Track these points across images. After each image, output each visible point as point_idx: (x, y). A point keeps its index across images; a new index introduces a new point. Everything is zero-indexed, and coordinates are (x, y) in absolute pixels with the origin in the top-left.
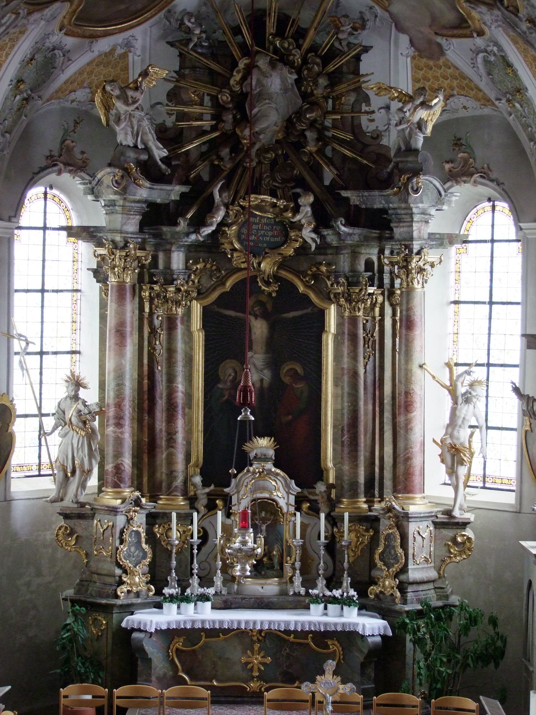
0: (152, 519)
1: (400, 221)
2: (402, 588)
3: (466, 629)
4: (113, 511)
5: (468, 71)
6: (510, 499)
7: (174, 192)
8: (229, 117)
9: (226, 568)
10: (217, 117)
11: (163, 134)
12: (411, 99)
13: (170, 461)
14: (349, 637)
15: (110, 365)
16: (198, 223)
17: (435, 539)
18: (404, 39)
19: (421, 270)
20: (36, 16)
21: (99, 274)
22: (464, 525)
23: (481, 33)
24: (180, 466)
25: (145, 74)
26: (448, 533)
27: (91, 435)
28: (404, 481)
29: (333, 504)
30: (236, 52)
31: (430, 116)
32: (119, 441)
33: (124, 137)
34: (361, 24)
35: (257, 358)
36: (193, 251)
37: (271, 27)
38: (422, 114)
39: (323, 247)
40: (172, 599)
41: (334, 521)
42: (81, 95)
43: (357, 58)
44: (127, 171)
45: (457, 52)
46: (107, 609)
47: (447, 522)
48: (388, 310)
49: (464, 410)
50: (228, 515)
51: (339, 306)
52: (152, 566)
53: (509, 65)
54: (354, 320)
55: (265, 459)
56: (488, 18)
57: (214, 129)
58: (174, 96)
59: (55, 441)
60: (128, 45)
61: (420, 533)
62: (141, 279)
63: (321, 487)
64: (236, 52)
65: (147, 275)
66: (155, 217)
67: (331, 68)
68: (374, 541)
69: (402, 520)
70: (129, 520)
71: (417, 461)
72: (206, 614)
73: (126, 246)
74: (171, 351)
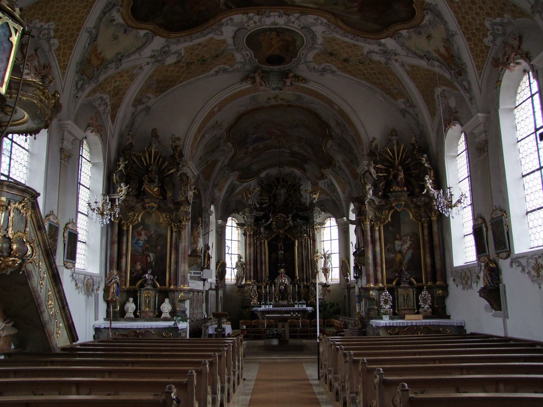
0: (259, 288)
1: (311, 218)
3: (331, 307)
4: (249, 285)
5: (323, 188)
10: (270, 200)
12: (312, 193)
13: (262, 275)
15: (248, 252)
16: (266, 221)
18: (309, 182)
19: (316, 229)
20: (232, 174)
21: (245, 234)
23: (326, 178)
24: (264, 276)
25: (254, 189)
27: (244, 269)
30: (273, 186)
32: (250, 269)
36: (266, 228)
37: (281, 180)
38: (315, 196)
39: (295, 226)
40: (263, 304)
41: (299, 287)
44: (251, 208)
45: (321, 184)
47: (325, 286)
49: (327, 260)
50: (275, 287)
51: (298, 239)
52: (258, 298)
54: (302, 242)
57: (269, 202)
60: (250, 185)
64: (273, 186)
65: (255, 234)
66: (257, 220)
68: (309, 291)
70: (253, 287)
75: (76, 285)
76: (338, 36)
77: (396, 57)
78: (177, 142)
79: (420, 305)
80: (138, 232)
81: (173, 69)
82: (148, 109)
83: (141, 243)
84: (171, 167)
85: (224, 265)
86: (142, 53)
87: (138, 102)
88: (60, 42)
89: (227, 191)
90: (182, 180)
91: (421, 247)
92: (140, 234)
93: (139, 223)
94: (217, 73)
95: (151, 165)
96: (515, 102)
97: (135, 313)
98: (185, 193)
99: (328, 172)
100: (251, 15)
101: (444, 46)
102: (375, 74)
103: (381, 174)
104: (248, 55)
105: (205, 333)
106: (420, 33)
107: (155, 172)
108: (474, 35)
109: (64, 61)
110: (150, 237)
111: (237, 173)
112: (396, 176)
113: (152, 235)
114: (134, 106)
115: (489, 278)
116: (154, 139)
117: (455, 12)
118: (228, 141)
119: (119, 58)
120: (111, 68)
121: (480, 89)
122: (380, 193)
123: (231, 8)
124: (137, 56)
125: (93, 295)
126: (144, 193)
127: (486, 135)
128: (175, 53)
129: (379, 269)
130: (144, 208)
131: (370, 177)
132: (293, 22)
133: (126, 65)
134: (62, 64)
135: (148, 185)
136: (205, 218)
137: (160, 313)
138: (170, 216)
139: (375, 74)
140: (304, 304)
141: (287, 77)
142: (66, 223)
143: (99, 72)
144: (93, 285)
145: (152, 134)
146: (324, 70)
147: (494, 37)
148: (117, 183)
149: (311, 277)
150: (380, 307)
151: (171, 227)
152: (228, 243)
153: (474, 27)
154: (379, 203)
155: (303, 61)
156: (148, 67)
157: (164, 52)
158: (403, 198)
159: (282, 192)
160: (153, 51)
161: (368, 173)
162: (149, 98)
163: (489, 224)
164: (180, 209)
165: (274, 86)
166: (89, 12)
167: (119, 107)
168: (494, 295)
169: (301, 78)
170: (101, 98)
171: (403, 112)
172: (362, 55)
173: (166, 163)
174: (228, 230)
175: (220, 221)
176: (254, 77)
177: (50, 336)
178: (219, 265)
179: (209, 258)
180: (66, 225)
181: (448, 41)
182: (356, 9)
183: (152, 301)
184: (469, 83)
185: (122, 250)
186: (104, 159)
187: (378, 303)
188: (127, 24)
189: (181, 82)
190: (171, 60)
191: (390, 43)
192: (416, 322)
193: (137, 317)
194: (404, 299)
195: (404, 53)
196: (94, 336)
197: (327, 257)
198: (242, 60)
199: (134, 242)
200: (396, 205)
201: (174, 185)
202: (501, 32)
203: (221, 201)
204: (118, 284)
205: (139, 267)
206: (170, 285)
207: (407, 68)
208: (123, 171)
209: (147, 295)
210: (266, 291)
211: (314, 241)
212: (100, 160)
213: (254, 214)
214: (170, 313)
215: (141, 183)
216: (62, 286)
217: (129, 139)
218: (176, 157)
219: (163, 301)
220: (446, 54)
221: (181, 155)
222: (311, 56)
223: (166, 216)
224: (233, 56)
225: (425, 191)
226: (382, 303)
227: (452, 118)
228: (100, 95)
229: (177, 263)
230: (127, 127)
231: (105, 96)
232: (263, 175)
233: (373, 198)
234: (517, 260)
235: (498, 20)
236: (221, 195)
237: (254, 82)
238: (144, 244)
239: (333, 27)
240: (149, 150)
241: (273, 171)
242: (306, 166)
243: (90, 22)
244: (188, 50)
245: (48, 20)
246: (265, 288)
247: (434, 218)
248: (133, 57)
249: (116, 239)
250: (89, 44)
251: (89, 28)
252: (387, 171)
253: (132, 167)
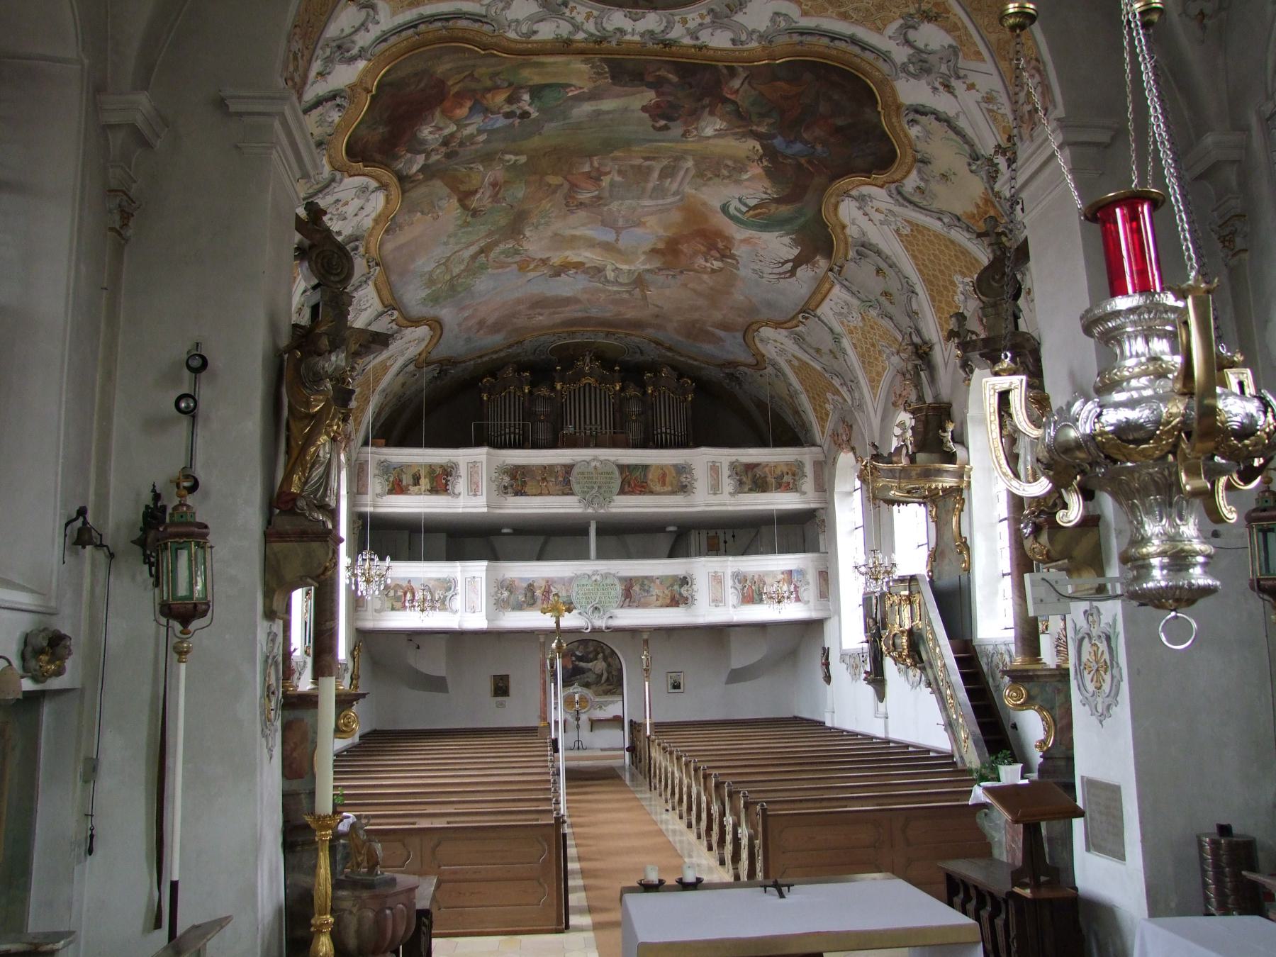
86: (951, 113)
100: (687, 41)
124: (962, 123)
128: (908, 42)
132: (587, 18)
160: (935, 89)
166: (925, 228)
182: (450, 83)
190: (932, 37)
244: (879, 23)
245: (953, 283)
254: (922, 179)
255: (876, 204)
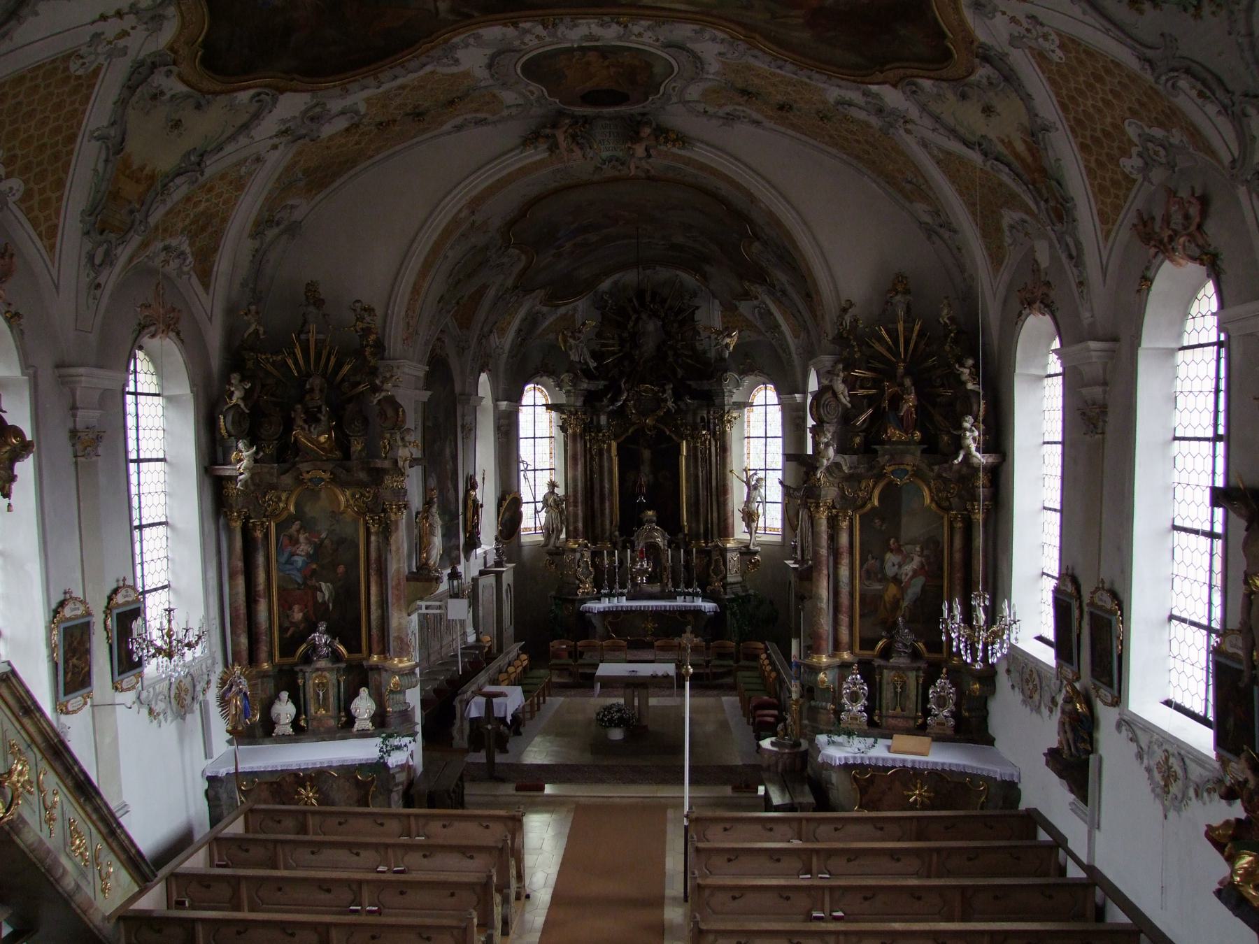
2: (724, 586)
4: (574, 550)
5: (750, 317)
6: (779, 539)
7: (601, 384)
8: (628, 345)
9: (633, 580)
11: (594, 355)
12: (722, 333)
14: (698, 612)
16: (613, 400)
17: (741, 561)
18: (717, 302)
21: (563, 428)
22: (755, 553)
23: (756, 298)
25: (584, 324)
26: (748, 557)
27: (561, 512)
28: (725, 530)
29: (687, 545)
31: (732, 341)
32: (576, 515)
33: (574, 357)
34: (694, 295)
35: (646, 469)
36: (611, 415)
37: (648, 299)
38: (728, 340)
39: (679, 411)
40: (605, 595)
42: (551, 336)
43: (693, 312)
44: (576, 374)
45: (744, 308)
46: (573, 601)
47: (746, 552)
48: (713, 443)
49: (754, 493)
50: (633, 551)
53: (772, 314)
54: (695, 448)
55: (651, 521)
56: (760, 290)
57: (620, 351)
58: (599, 335)
59: (543, 515)
60: (575, 309)
61: (733, 558)
62: (584, 431)
63: (681, 536)
66: (591, 399)
67: (680, 318)
69: (724, 551)
70: (582, 556)
71: (730, 521)
72: (624, 602)
73: (576, 413)
74: (601, 467)
75: (151, 711)
76: (757, 63)
77: (909, 126)
78: (368, 319)
79: (930, 710)
80: (290, 537)
81: (343, 141)
82: (293, 229)
83: (299, 560)
84: (358, 378)
85: (517, 502)
86: (253, 133)
87: (261, 226)
88: (26, 182)
89: (519, 331)
90: (383, 414)
91: (946, 574)
92: (294, 541)
93: (290, 515)
94: (458, 128)
95: (309, 375)
96: (1180, 335)
97: (295, 723)
98: (391, 448)
99: (757, 289)
101: (1025, 141)
102: (858, 142)
103: (861, 392)
104: (532, 93)
105: (462, 715)
106: (964, 97)
107: (321, 391)
108: (1096, 140)
109: (47, 219)
110: (318, 547)
111: (540, 293)
112: (896, 401)
113: (322, 541)
114: (257, 233)
115: (1070, 735)
116: (312, 309)
117: (1052, 82)
118: (507, 247)
119: (195, 162)
120: (178, 187)
121: (1104, 272)
122: (858, 440)
123: (469, 16)
124: (243, 140)
125: (197, 707)
126: (297, 448)
127: (1105, 392)
128: (343, 113)
129: (844, 619)
130: (299, 481)
131: (833, 404)
133: (213, 167)
134: (42, 228)
135: (303, 429)
136: (463, 416)
137: (351, 720)
138: (362, 495)
139: (858, 142)
140: (697, 595)
141: (635, 137)
142: (108, 592)
143: (144, 208)
144: (194, 686)
145: (307, 297)
146: (730, 118)
147: (1146, 164)
148: (230, 435)
149: (715, 532)
150: (839, 709)
151: (366, 523)
152: (525, 450)
153: (1099, 127)
154: (850, 468)
155: (674, 99)
156: (277, 153)
157: (312, 119)
158: (909, 459)
159: (651, 327)
160: (283, 121)
161: (828, 395)
162: (292, 207)
163: (1086, 609)
164: (383, 481)
165: (605, 154)
166: (88, 98)
167: (216, 250)
168: (1075, 764)
169: (673, 136)
170: (167, 249)
171: (930, 232)
172: (825, 102)
173: (346, 368)
174: (525, 416)
175: (503, 405)
176: (554, 136)
177: (85, 912)
178: (505, 504)
179: (477, 507)
180: (110, 599)
181: (1035, 133)
182: (801, 21)
183: (332, 693)
184: (1078, 244)
185: (256, 585)
186: (193, 384)
187: (836, 697)
188: (200, 91)
189: (371, 157)
191: (892, 97)
192: (913, 762)
193: (300, 731)
194: (896, 693)
195: (927, 122)
196: (206, 792)
197: (753, 487)
198: (521, 101)
199: (283, 560)
200: (893, 473)
201: (366, 421)
202: (1163, 160)
203: (505, 356)
204: (245, 694)
205: (298, 616)
206: (370, 652)
207: (936, 152)
208: (242, 405)
209: (321, 677)
210: (612, 562)
211: (724, 450)
212: (184, 389)
213: (585, 385)
214: (373, 719)
215: (289, 425)
216: (102, 799)
217: (249, 324)
218: (365, 353)
219: (356, 694)
220: (1030, 160)
221: (380, 347)
222: (694, 92)
223: (353, 496)
224: (494, 96)
225: (960, 459)
226: (845, 700)
227: (1036, 294)
228: (161, 245)
229: (383, 604)
230: (244, 285)
231: (174, 242)
232: (606, 285)
233: (839, 459)
234: (1132, 726)
235: (1158, 133)
236: (504, 342)
237: (554, 147)
238: (306, 564)
239: (743, 47)
240: (303, 337)
241: (630, 277)
242: (707, 268)
243: (98, 114)
246: (611, 554)
247: (980, 517)
248: (229, 148)
249: (240, 564)
250: (106, 161)
251: (98, 129)
252: (876, 383)
253: (263, 386)
254: (173, 96)
255: (139, 35)
